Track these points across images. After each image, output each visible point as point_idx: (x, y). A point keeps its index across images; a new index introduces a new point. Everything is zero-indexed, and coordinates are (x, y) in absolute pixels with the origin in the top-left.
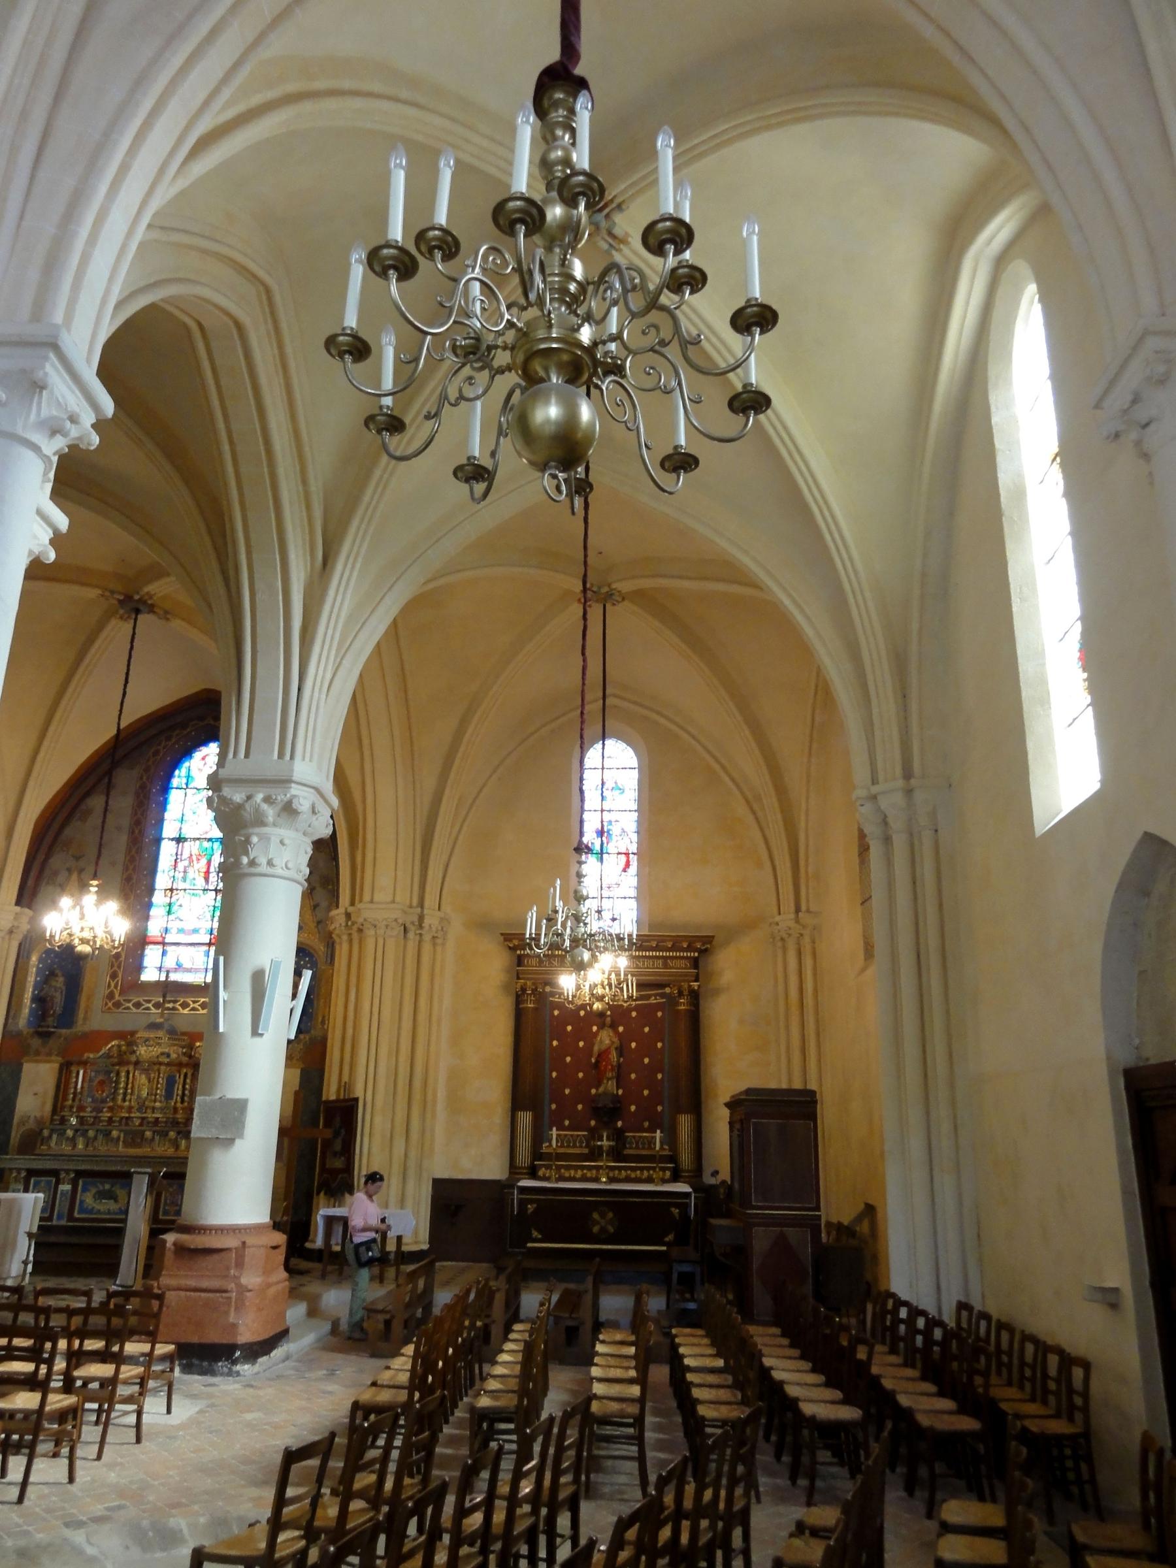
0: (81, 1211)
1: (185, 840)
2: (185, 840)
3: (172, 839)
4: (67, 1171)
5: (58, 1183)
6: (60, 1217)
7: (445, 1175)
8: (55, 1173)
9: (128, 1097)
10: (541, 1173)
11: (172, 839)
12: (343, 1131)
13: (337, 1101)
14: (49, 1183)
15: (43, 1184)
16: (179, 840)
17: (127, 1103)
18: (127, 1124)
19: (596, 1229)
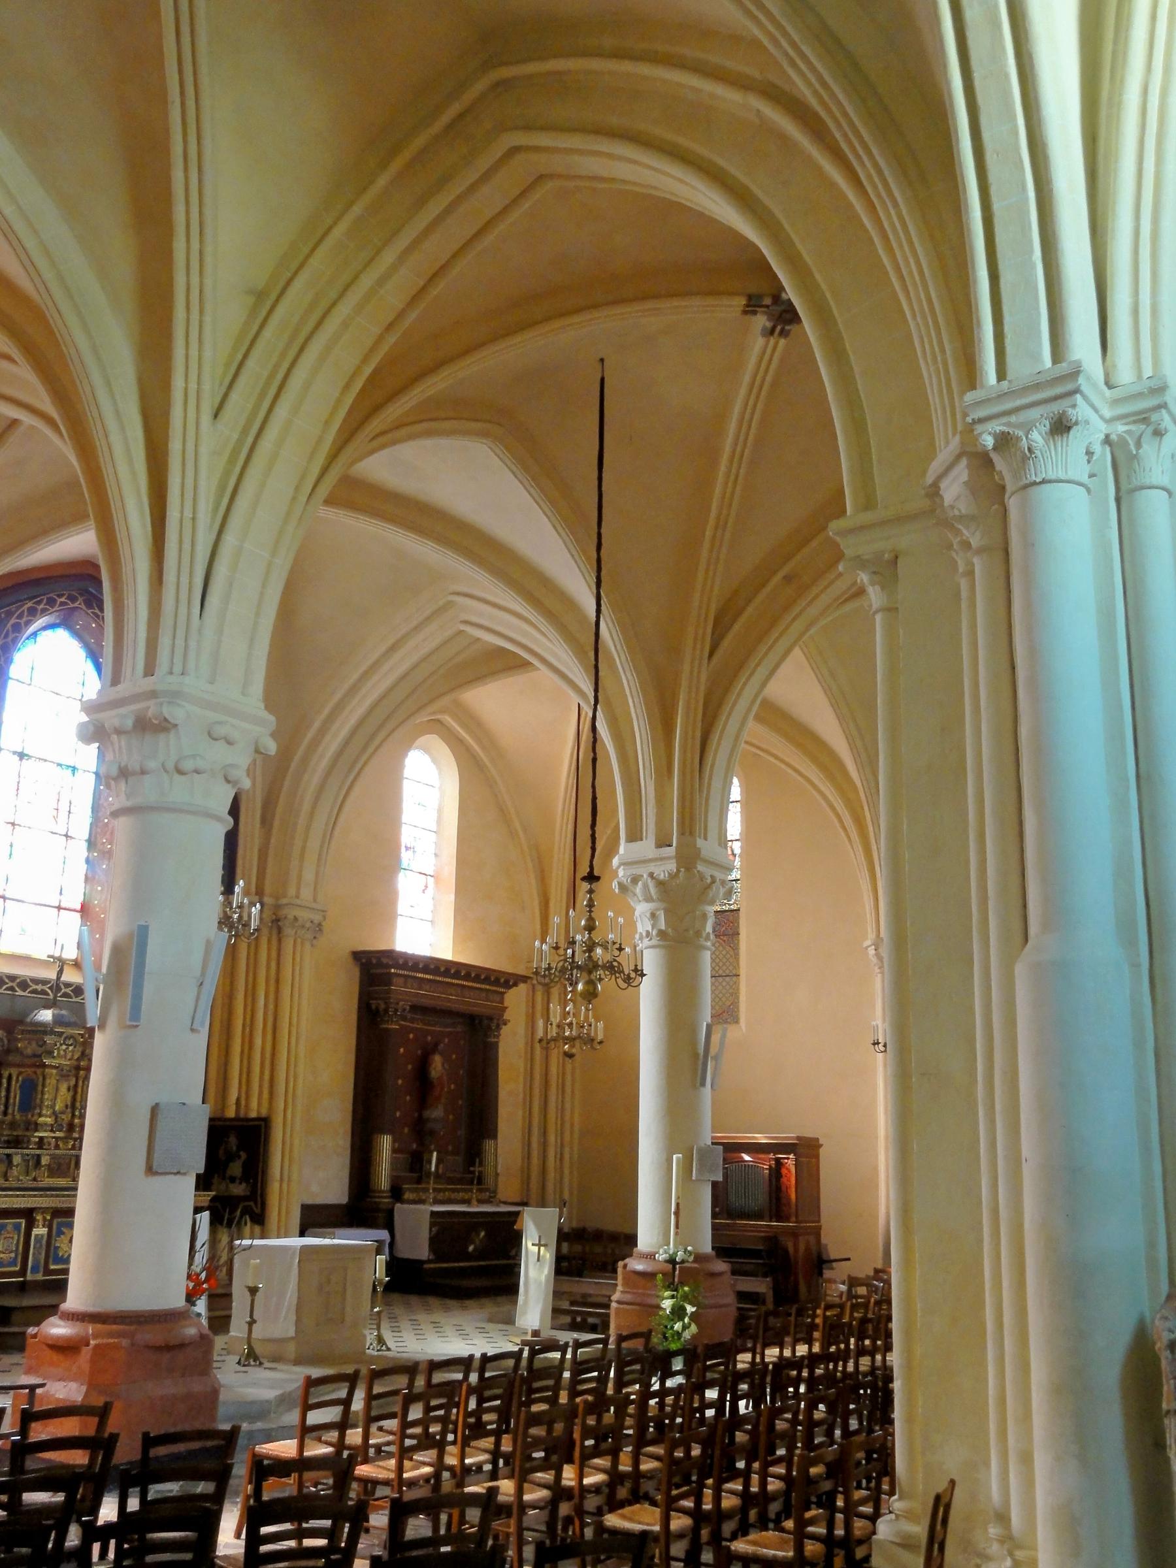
0: (14, 1263)
1: (29, 757)
2: (29, 757)
3: (14, 753)
4: (44, 1210)
5: (30, 1225)
6: (35, 1269)
7: (310, 1202)
8: (28, 1214)
9: (10, 1111)
10: (407, 1195)
11: (14, 753)
12: (243, 1155)
13: (237, 1119)
14: (17, 1227)
15: (9, 1228)
16: (22, 756)
17: (9, 1118)
18: (57, 1147)
19: (471, 1248)
